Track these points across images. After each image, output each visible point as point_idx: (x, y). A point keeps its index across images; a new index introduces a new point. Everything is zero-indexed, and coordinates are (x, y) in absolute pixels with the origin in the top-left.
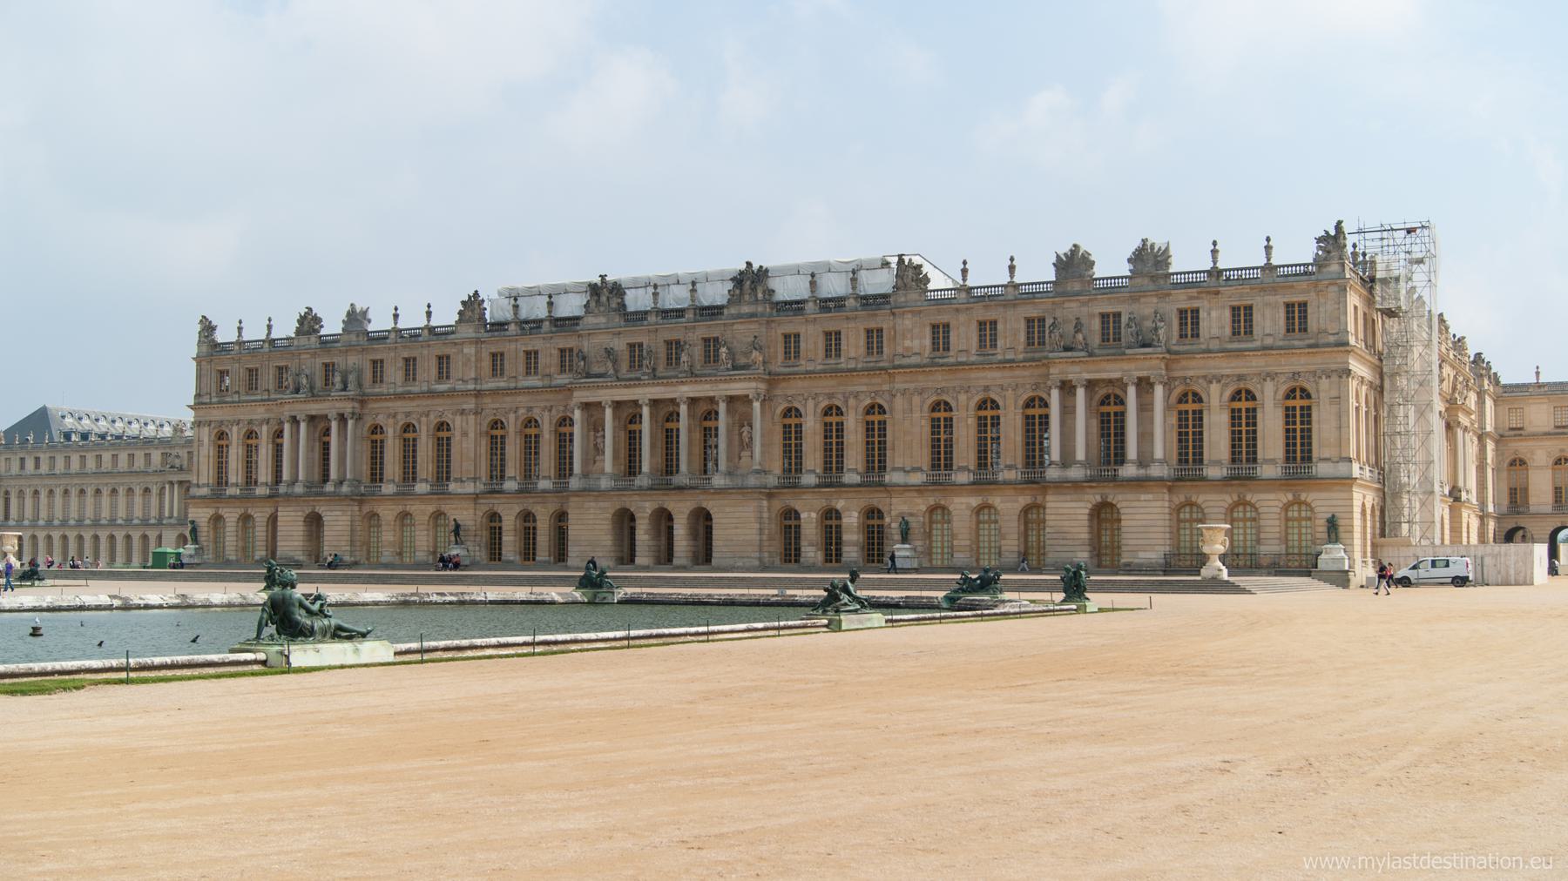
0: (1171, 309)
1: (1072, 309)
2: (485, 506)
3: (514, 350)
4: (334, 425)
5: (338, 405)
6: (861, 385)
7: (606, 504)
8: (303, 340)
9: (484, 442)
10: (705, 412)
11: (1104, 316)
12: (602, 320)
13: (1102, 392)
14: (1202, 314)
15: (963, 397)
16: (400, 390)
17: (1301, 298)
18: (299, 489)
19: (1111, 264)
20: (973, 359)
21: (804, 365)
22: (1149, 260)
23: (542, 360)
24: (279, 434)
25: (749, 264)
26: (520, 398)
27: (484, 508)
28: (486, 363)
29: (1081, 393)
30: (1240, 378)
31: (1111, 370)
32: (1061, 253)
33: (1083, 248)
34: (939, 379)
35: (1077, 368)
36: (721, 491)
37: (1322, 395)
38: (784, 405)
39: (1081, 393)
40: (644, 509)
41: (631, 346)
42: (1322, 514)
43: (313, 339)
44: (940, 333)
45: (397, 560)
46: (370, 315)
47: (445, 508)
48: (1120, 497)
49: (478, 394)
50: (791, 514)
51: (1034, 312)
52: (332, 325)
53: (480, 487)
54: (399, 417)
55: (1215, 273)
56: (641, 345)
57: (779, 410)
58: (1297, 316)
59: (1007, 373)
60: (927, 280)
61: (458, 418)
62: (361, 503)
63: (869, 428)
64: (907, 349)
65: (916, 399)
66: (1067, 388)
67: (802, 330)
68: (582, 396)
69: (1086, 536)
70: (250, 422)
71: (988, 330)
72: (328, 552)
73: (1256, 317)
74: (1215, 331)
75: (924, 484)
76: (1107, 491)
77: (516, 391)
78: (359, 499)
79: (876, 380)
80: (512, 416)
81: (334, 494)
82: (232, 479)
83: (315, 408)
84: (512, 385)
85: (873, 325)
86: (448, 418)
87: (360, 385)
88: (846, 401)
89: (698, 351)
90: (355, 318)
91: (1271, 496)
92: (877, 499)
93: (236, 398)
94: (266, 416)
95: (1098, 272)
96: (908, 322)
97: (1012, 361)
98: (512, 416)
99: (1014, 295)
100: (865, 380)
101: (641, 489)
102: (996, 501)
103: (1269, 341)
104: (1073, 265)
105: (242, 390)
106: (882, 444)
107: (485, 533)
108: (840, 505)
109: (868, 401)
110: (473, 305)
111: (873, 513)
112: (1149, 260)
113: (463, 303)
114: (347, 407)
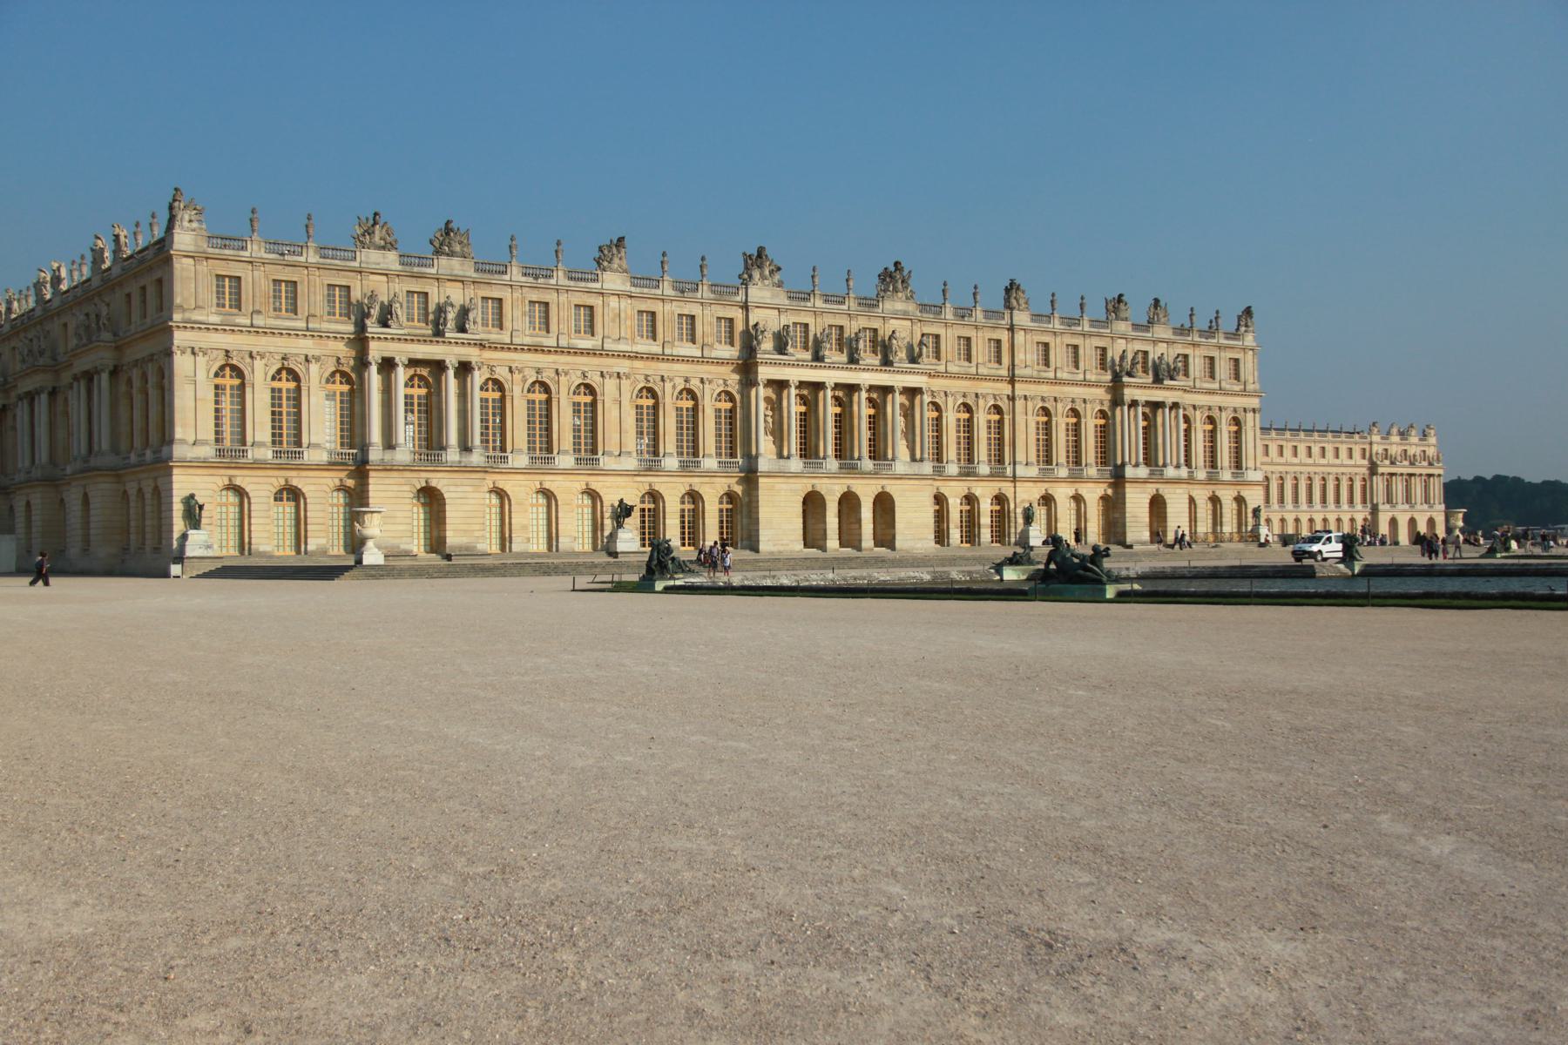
2: (644, 483)
6: (985, 388)
7: (799, 486)
16: (528, 340)
26: (677, 366)
27: (644, 483)
31: (1157, 395)
34: (1044, 390)
36: (901, 477)
40: (832, 491)
42: (1251, 506)
47: (597, 484)
49: (636, 356)
50: (940, 499)
59: (1087, 390)
67: (941, 331)
80: (668, 385)
84: (667, 351)
86: (594, 379)
94: (317, 353)
103: (1224, 384)
108: (978, 492)
111: (1000, 499)
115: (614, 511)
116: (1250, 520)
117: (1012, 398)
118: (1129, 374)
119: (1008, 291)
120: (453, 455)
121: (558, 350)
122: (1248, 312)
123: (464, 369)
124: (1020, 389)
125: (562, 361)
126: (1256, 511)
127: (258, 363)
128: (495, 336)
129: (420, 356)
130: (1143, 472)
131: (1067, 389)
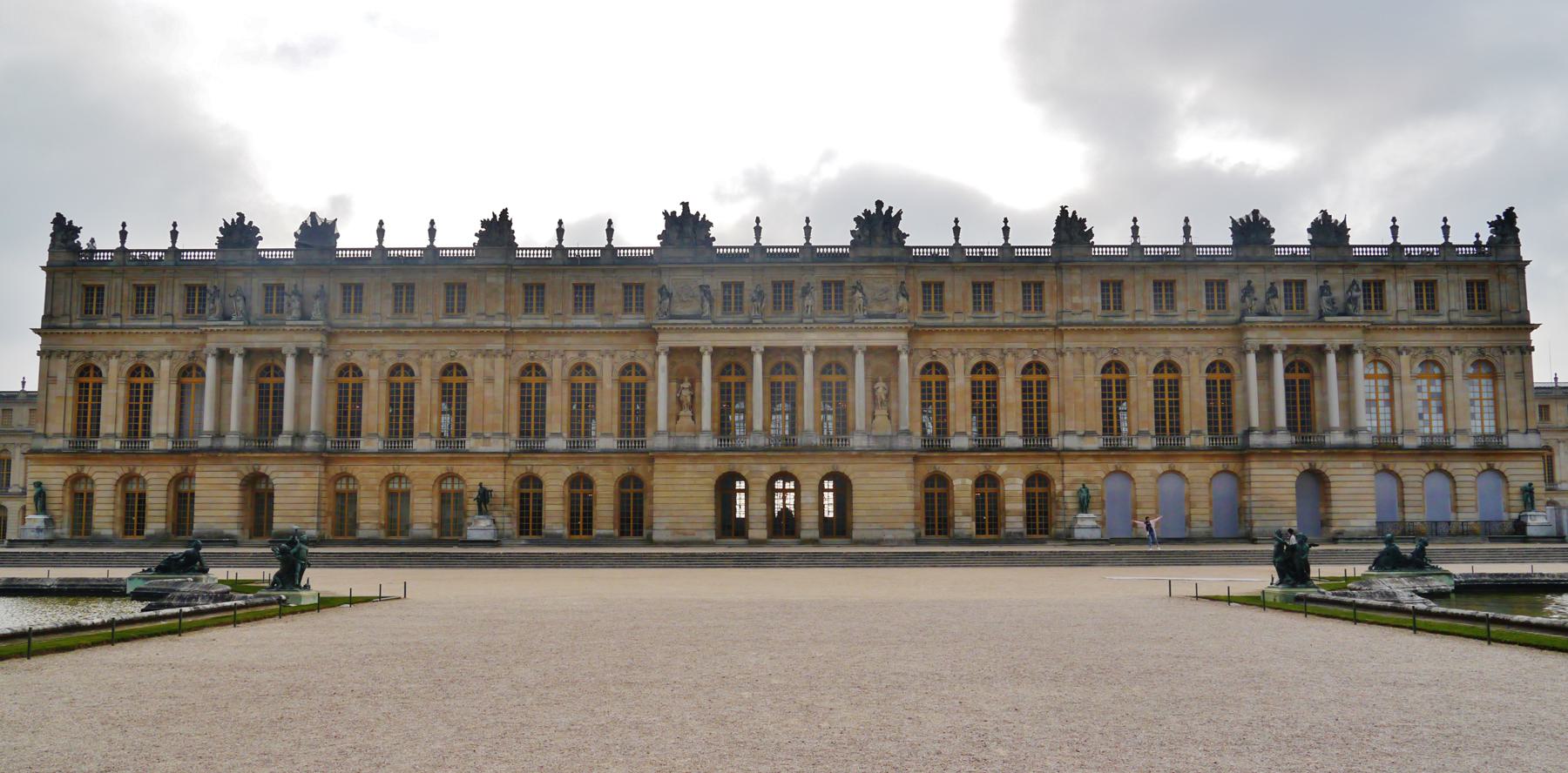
4: (290, 366)
5: (297, 337)
7: (710, 467)
8: (232, 255)
9: (515, 390)
10: (834, 363)
11: (1287, 283)
12: (686, 253)
13: (1291, 359)
14: (1389, 287)
15: (1141, 359)
17: (1482, 277)
18: (232, 442)
20: (1151, 319)
21: (950, 318)
22: (1328, 232)
23: (600, 297)
24: (189, 373)
25: (879, 204)
26: (568, 340)
27: (518, 469)
28: (519, 297)
29: (1278, 359)
30: (1429, 350)
31: (1312, 338)
32: (1237, 218)
33: (1263, 214)
34: (1116, 340)
35: (1276, 334)
37: (1508, 370)
38: (928, 360)
39: (1278, 359)
41: (726, 285)
43: (248, 253)
45: (382, 534)
46: (339, 229)
47: (459, 469)
48: (1329, 465)
49: (511, 333)
50: (942, 481)
51: (1216, 275)
52: (278, 238)
53: (512, 445)
54: (387, 356)
55: (1395, 247)
56: (740, 285)
57: (919, 367)
58: (1478, 294)
59: (1190, 336)
60: (1090, 234)
61: (479, 360)
62: (327, 463)
63: (1026, 388)
64: (1075, 306)
65: (1089, 358)
66: (1266, 353)
68: (667, 340)
69: (1293, 504)
70: (140, 355)
72: (280, 523)
73: (1442, 293)
74: (1402, 304)
75: (1101, 449)
76: (1313, 459)
77: (563, 331)
78: (324, 456)
79: (1037, 338)
80: (557, 361)
81: (292, 450)
82: (106, 426)
83: (259, 341)
84: (558, 323)
85: (1033, 278)
86: (464, 359)
87: (326, 315)
88: (1003, 359)
89: (817, 294)
90: (317, 234)
91: (1467, 465)
92: (1048, 466)
93: (116, 323)
94: (169, 348)
95: (1278, 238)
96: (1073, 278)
97: (1194, 324)
98: (557, 361)
99: (1186, 258)
100: (1025, 337)
101: (754, 449)
102: (1185, 467)
103: (1455, 317)
104: (1253, 231)
105: (128, 312)
106: (1044, 407)
107: (516, 501)
108: (1001, 470)
109: (1029, 359)
110: (498, 230)
111: (1038, 481)
112: (1328, 232)
113: (484, 223)
114: (314, 341)
115: (476, 495)
116: (1517, 502)
118: (1265, 314)
119: (1059, 220)
120: (283, 441)
121: (421, 331)
122: (1510, 214)
123: (303, 356)
124: (1070, 342)
126: (1528, 492)
127: (114, 362)
128: (353, 322)
129: (257, 346)
130: (1283, 439)
131: (1154, 337)
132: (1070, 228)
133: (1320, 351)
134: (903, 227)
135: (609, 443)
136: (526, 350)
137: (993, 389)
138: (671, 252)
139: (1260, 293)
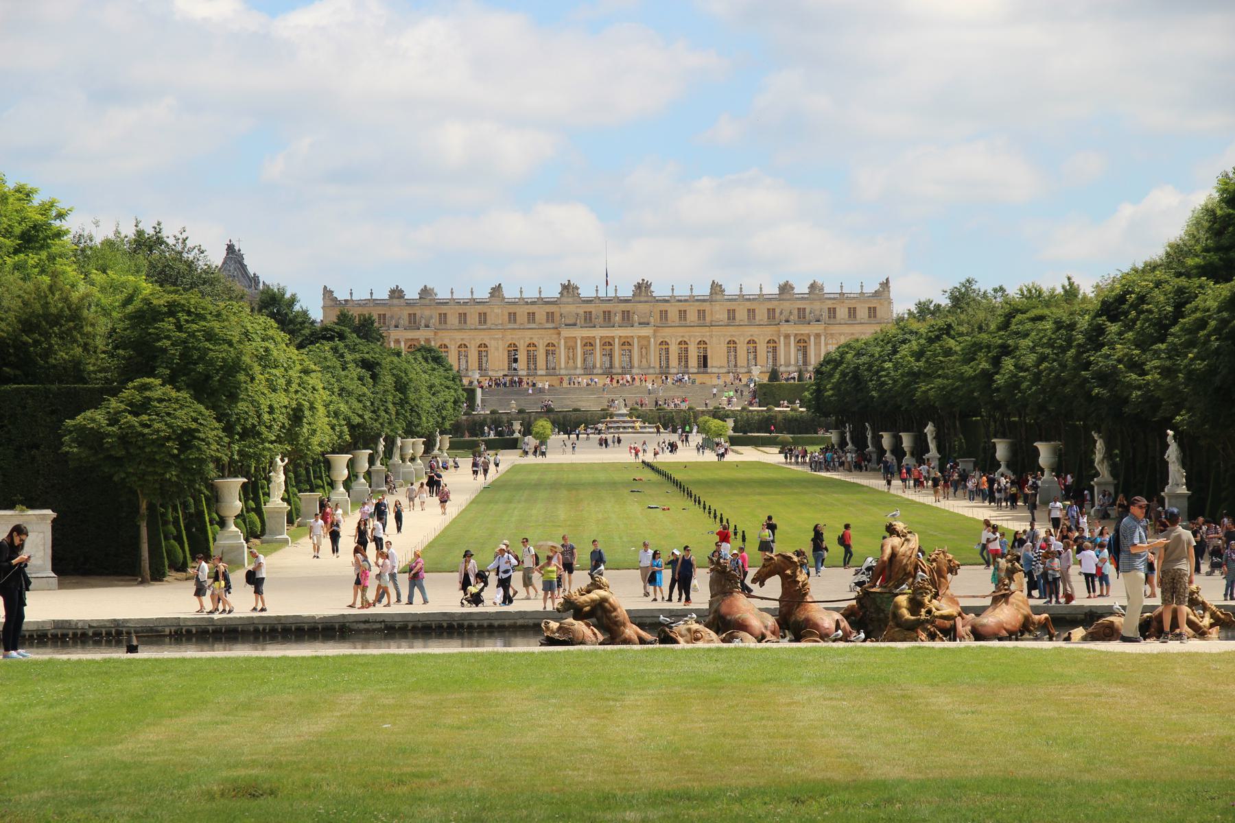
0: (826, 307)
1: (787, 305)
3: (522, 311)
8: (396, 301)
12: (570, 300)
19: (801, 288)
23: (537, 316)
28: (507, 317)
44: (732, 314)
66: (787, 336)
71: (752, 312)
73: (858, 312)
90: (425, 292)
95: (796, 291)
96: (717, 307)
99: (761, 298)
104: (785, 288)
117: (711, 336)
125: (473, 333)
132: (716, 288)
133: (809, 336)
134: (652, 288)
135: (543, 372)
136: (511, 337)
137: (686, 350)
138: (564, 299)
139: (786, 313)
